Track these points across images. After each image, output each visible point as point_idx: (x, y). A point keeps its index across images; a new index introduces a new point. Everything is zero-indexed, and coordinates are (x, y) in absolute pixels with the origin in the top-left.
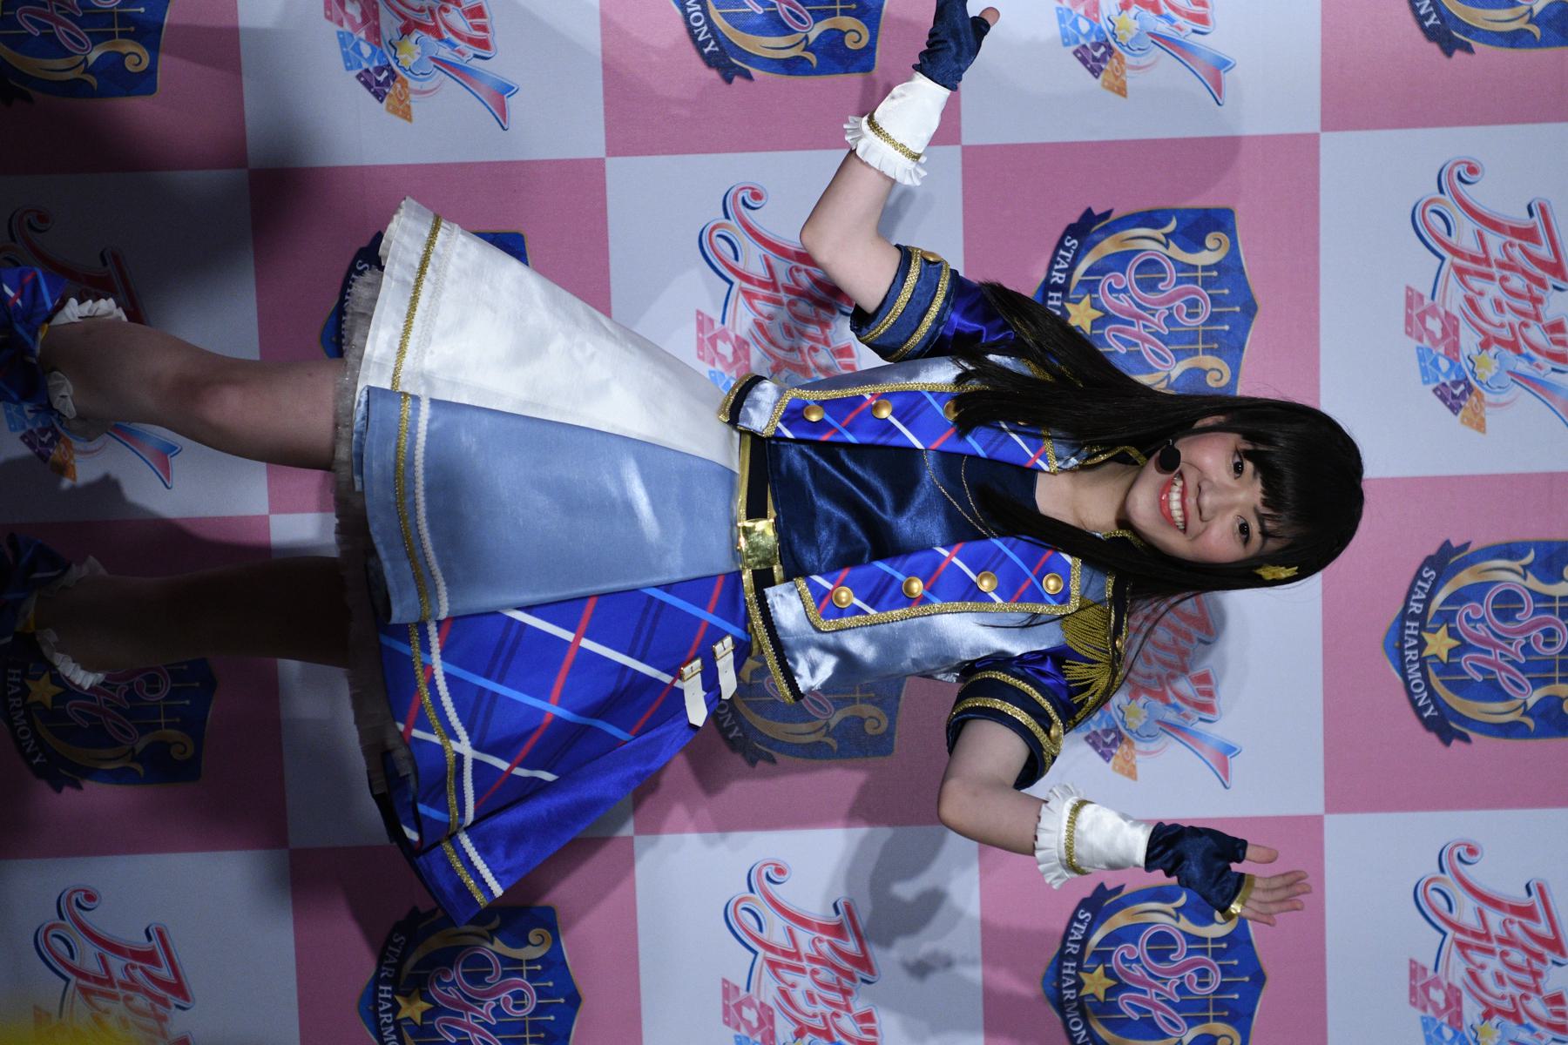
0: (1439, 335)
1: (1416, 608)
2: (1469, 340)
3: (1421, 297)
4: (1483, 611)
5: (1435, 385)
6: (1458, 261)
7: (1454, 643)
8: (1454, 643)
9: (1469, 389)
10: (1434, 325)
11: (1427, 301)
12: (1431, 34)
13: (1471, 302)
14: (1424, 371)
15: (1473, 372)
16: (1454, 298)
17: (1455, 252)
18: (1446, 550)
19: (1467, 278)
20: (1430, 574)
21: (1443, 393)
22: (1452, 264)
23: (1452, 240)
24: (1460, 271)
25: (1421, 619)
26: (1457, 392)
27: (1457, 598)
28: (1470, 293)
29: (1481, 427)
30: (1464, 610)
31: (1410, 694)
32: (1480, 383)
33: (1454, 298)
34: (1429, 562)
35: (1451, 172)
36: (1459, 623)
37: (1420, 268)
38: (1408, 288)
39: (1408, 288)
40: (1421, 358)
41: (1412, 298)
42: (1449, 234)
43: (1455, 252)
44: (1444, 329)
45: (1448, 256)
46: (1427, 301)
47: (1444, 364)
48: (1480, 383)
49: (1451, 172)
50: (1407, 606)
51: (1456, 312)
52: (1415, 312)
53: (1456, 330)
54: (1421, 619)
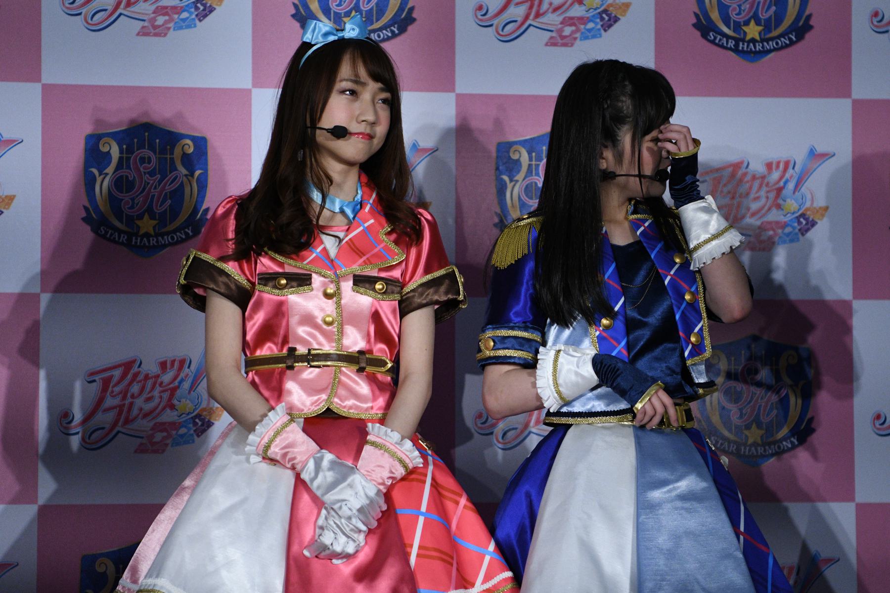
0: (573, 28)
1: (731, 44)
2: (577, 11)
3: (552, 38)
4: (735, 6)
5: (602, 31)
6: (531, 17)
7: (752, 23)
8: (752, 23)
9: (605, 11)
10: (568, 31)
11: (554, 34)
12: (403, 30)
13: (556, 10)
14: (594, 37)
15: (595, 9)
16: (553, 19)
17: (527, 18)
18: (698, 26)
19: (541, 11)
20: (711, 36)
21: (607, 27)
22: (533, 20)
23: (520, 19)
24: (538, 15)
25: (737, 41)
26: (607, 18)
27: (726, 21)
28: (550, 10)
29: (627, 6)
30: (734, 17)
31: (782, 48)
32: (602, 5)
33: (553, 19)
34: (705, 36)
35: (481, 20)
36: (741, 19)
37: (534, 38)
38: (547, 45)
39: (547, 45)
40: (586, 38)
41: (552, 43)
42: (516, 21)
43: (527, 18)
44: (570, 25)
45: (529, 22)
46: (554, 34)
47: (590, 25)
48: (602, 5)
49: (481, 20)
50: (730, 49)
51: (561, 19)
52: (560, 41)
53: (571, 18)
54: (737, 41)
